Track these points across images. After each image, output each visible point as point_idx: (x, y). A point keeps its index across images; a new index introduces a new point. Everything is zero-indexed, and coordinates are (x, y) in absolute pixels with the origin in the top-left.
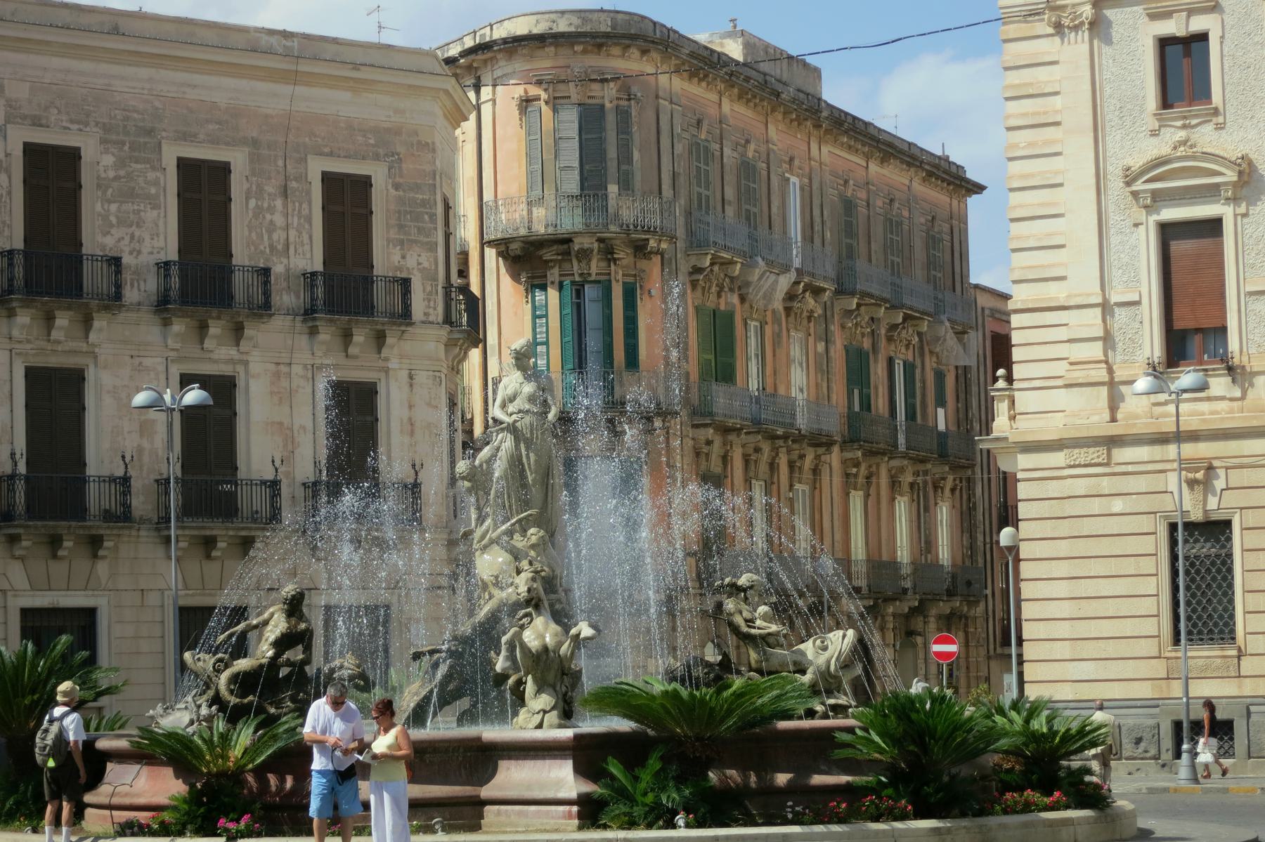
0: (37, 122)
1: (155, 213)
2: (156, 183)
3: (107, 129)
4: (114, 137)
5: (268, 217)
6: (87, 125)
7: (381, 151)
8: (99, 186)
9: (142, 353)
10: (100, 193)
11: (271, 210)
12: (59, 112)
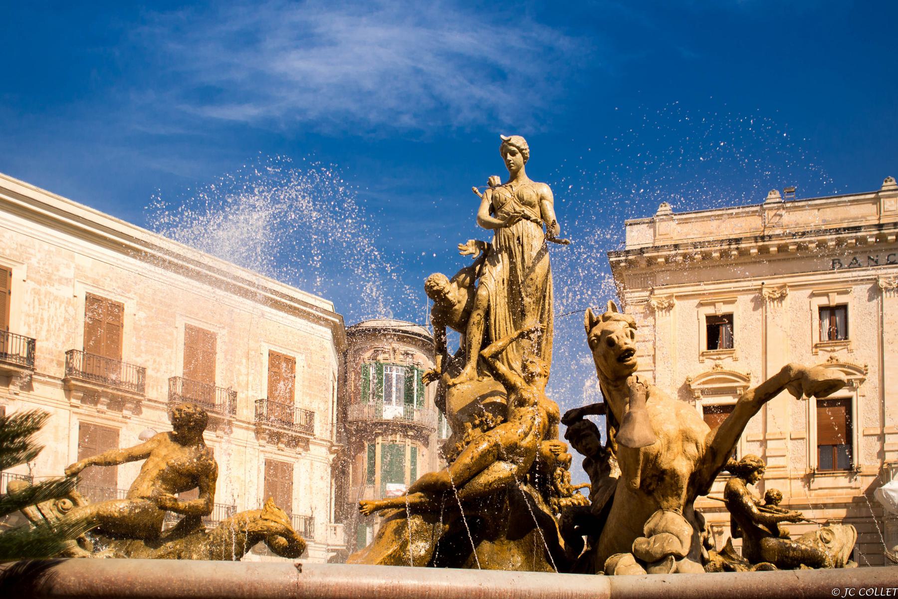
1: (169, 351)
2: (171, 334)
5: (237, 366)
7: (302, 347)
11: (240, 363)
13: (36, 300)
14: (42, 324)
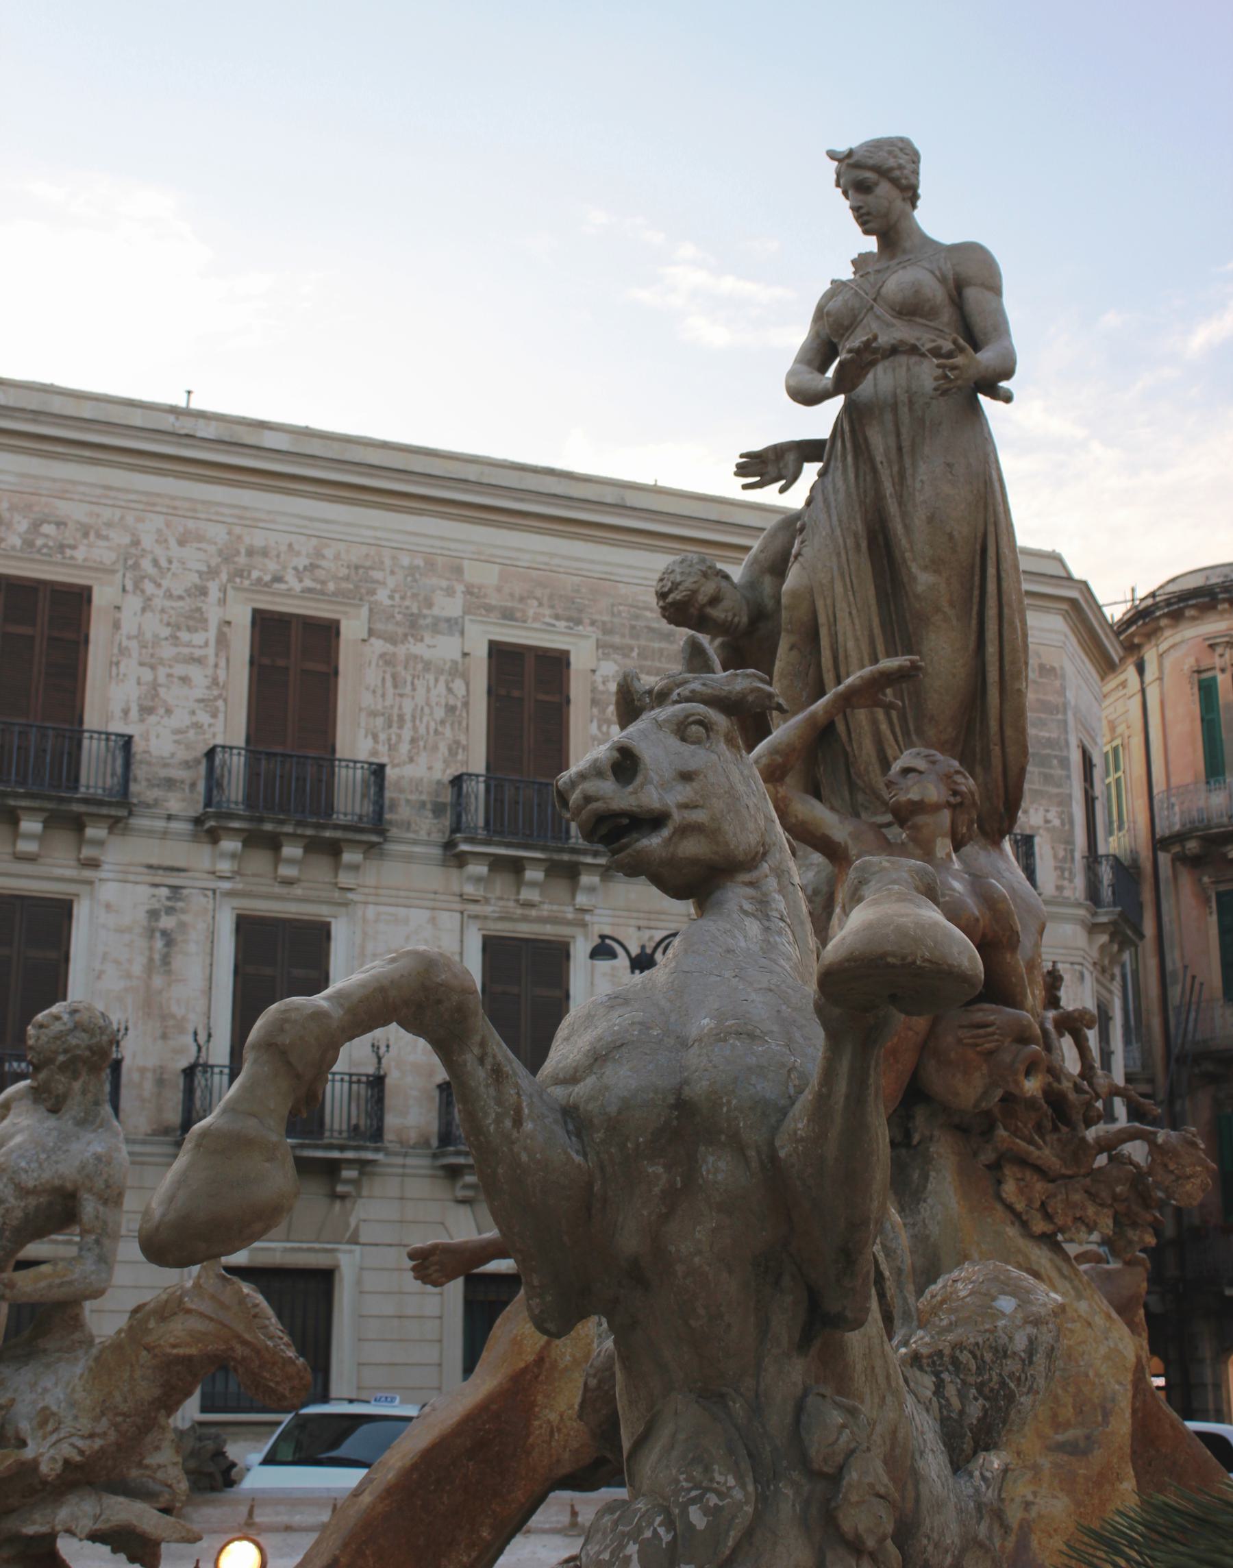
0: (508, 615)
3: (607, 630)
4: (617, 640)
6: (579, 622)
8: (594, 702)
9: (653, 924)
10: (595, 711)
12: (541, 605)
13: (388, 677)
14: (401, 727)
